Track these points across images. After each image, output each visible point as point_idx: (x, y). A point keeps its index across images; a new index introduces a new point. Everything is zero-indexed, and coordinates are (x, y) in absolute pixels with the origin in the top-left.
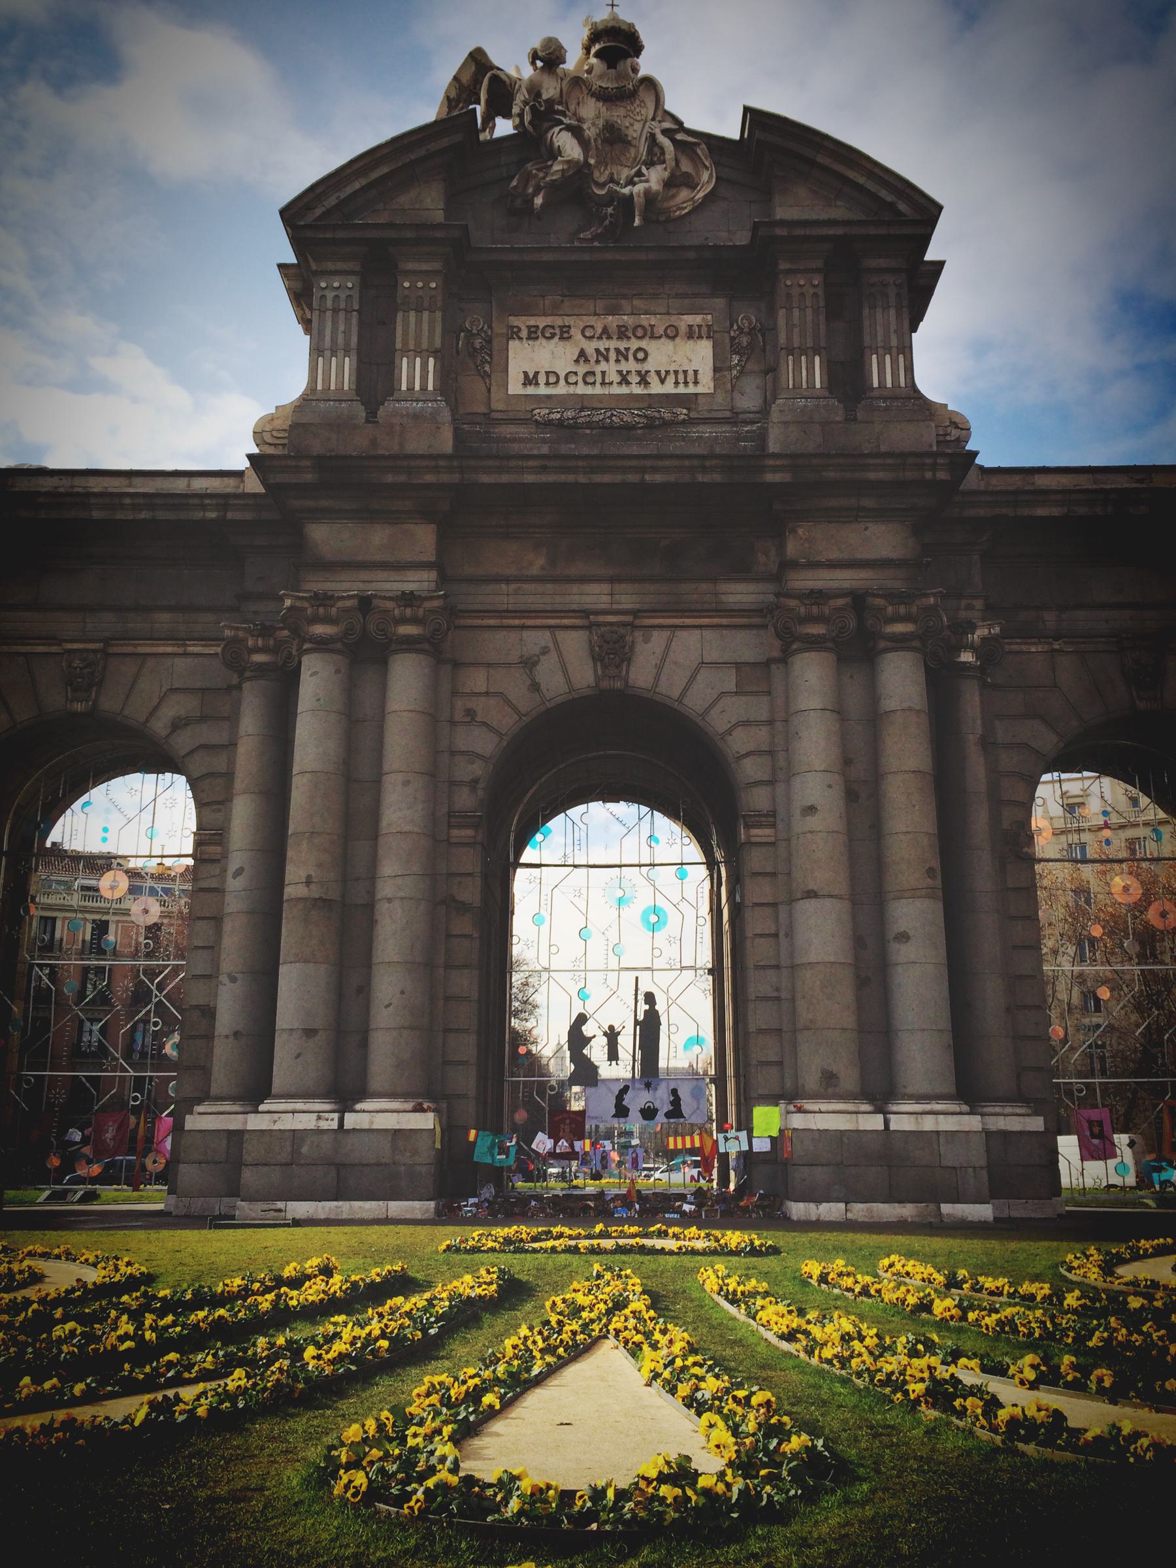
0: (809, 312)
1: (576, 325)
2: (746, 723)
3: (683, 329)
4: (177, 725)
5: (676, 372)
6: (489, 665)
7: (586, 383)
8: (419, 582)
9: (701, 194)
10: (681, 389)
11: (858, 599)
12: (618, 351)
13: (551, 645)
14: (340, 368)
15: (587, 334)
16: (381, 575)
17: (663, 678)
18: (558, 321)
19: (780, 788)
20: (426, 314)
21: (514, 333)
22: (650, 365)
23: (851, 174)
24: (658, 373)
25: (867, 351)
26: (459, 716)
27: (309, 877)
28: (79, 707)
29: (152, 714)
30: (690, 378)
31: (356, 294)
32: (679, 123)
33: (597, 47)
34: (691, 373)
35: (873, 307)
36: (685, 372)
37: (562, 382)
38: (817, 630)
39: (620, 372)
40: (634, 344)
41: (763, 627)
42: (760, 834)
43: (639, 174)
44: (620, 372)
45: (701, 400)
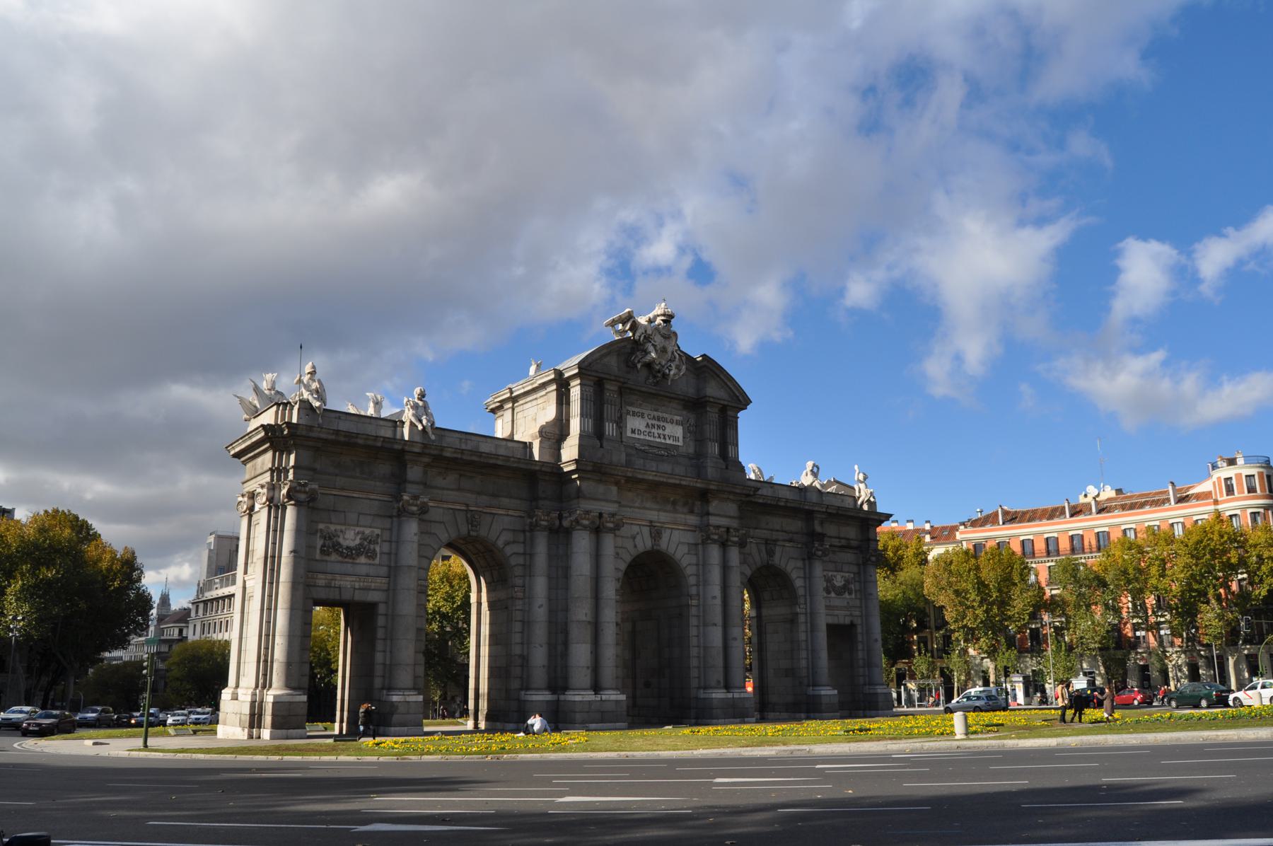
1: (646, 412)
2: (689, 564)
3: (675, 421)
4: (507, 543)
6: (622, 537)
10: (674, 443)
11: (728, 529)
14: (588, 422)
16: (603, 503)
18: (641, 411)
19: (701, 587)
21: (628, 413)
22: (666, 432)
23: (728, 383)
28: (473, 534)
29: (497, 538)
32: (679, 348)
33: (663, 318)
35: (730, 428)
38: (716, 537)
41: (695, 531)
42: (694, 602)
43: (670, 366)
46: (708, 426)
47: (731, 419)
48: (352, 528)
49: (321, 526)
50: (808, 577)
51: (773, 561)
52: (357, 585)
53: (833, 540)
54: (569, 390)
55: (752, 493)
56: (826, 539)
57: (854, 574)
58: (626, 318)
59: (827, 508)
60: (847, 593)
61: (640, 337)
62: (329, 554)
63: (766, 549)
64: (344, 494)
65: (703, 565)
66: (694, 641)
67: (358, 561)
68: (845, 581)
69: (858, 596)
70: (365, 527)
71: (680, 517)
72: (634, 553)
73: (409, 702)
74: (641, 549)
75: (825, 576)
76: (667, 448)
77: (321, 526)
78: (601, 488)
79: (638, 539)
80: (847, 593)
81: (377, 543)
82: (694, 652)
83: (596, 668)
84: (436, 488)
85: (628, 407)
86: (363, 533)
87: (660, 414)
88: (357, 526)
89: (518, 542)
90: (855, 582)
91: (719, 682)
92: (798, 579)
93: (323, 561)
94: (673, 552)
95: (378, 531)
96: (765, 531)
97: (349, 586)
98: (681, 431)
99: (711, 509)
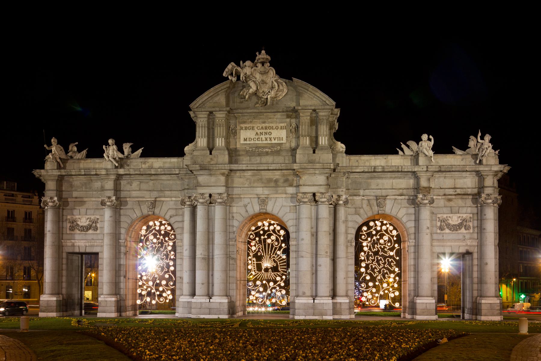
0: (306, 126)
3: (280, 127)
5: (278, 138)
9: (284, 94)
10: (279, 142)
12: (265, 132)
13: (250, 202)
15: (258, 128)
17: (274, 209)
21: (242, 128)
22: (272, 136)
24: (274, 138)
25: (319, 136)
26: (231, 218)
27: (201, 253)
29: (166, 214)
31: (206, 123)
34: (281, 138)
36: (280, 138)
37: (252, 140)
39: (265, 138)
40: (268, 131)
44: (265, 138)
45: (283, 145)
47: (321, 118)
48: (85, 216)
49: (69, 217)
50: (417, 220)
53: (446, 190)
60: (463, 229)
62: (73, 230)
64: (79, 200)
67: (88, 233)
68: (461, 220)
69: (476, 229)
72: (245, 215)
74: (251, 212)
76: (273, 145)
77: (69, 217)
78: (213, 179)
80: (463, 229)
81: (98, 223)
85: (241, 125)
87: (267, 125)
94: (277, 213)
95: (98, 217)
96: (376, 190)
97: (83, 245)
98: (285, 133)
99: (301, 182)
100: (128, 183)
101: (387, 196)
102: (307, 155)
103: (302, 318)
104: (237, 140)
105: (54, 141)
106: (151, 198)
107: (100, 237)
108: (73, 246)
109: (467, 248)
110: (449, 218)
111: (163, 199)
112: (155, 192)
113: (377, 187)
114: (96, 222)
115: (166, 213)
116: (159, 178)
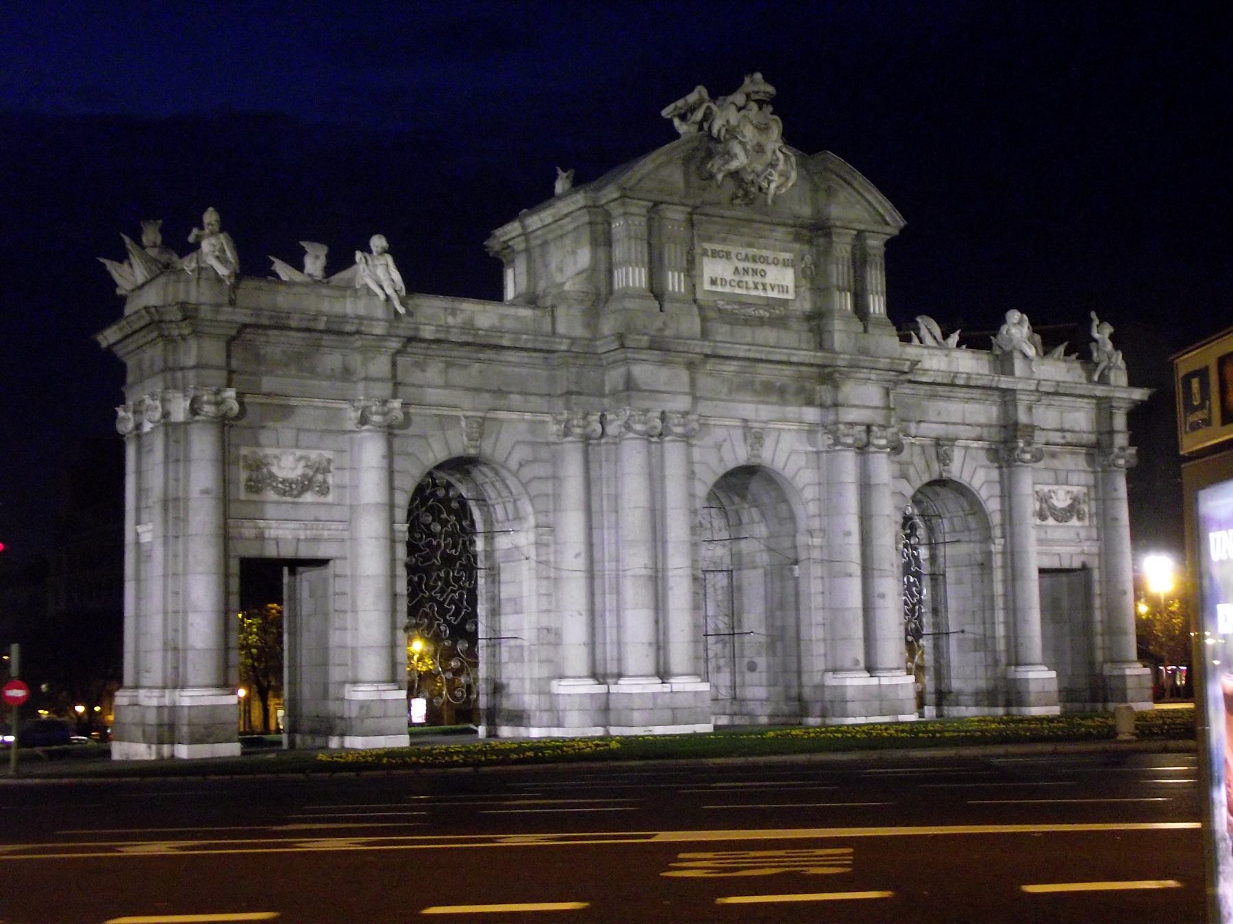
1: (734, 250)
7: (739, 287)
8: (683, 403)
14: (640, 272)
18: (726, 248)
20: (678, 246)
21: (705, 253)
22: (769, 279)
24: (771, 285)
30: (785, 290)
34: (785, 287)
35: (871, 267)
38: (850, 441)
40: (759, 266)
43: (771, 174)
45: (790, 303)
46: (835, 266)
48: (291, 450)
49: (244, 451)
50: (1007, 494)
51: (950, 472)
52: (302, 535)
53: (1051, 433)
54: (610, 224)
55: (906, 369)
56: (1037, 433)
57: (1088, 487)
58: (695, 103)
59: (1038, 384)
61: (719, 131)
63: (937, 453)
65: (829, 486)
66: (817, 601)
67: (300, 500)
70: (307, 448)
71: (792, 411)
72: (721, 471)
73: (385, 701)
75: (1037, 492)
76: (770, 303)
77: (244, 451)
78: (664, 373)
79: (726, 447)
81: (329, 471)
82: (818, 617)
83: (660, 646)
84: (414, 385)
86: (306, 458)
88: (297, 446)
89: (542, 461)
90: (1089, 499)
91: (857, 662)
92: (992, 500)
93: (249, 501)
95: (328, 454)
96: (938, 426)
97: (290, 537)
100: (416, 364)
101: (957, 439)
102: (853, 336)
103: (861, 720)
104: (697, 281)
105: (210, 217)
106: (477, 410)
107: (343, 513)
108: (261, 537)
109: (1083, 558)
110: (1053, 495)
111: (502, 415)
112: (487, 395)
113: (939, 419)
114: (326, 471)
115: (510, 454)
116: (501, 358)
